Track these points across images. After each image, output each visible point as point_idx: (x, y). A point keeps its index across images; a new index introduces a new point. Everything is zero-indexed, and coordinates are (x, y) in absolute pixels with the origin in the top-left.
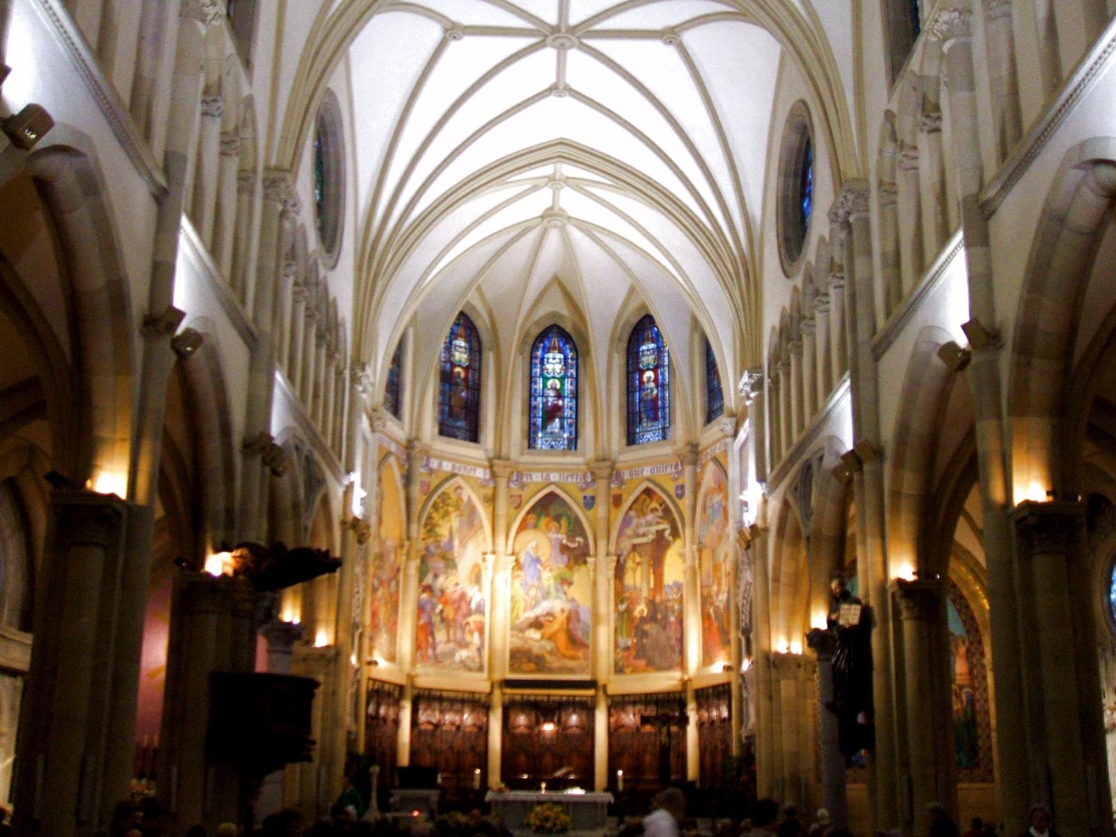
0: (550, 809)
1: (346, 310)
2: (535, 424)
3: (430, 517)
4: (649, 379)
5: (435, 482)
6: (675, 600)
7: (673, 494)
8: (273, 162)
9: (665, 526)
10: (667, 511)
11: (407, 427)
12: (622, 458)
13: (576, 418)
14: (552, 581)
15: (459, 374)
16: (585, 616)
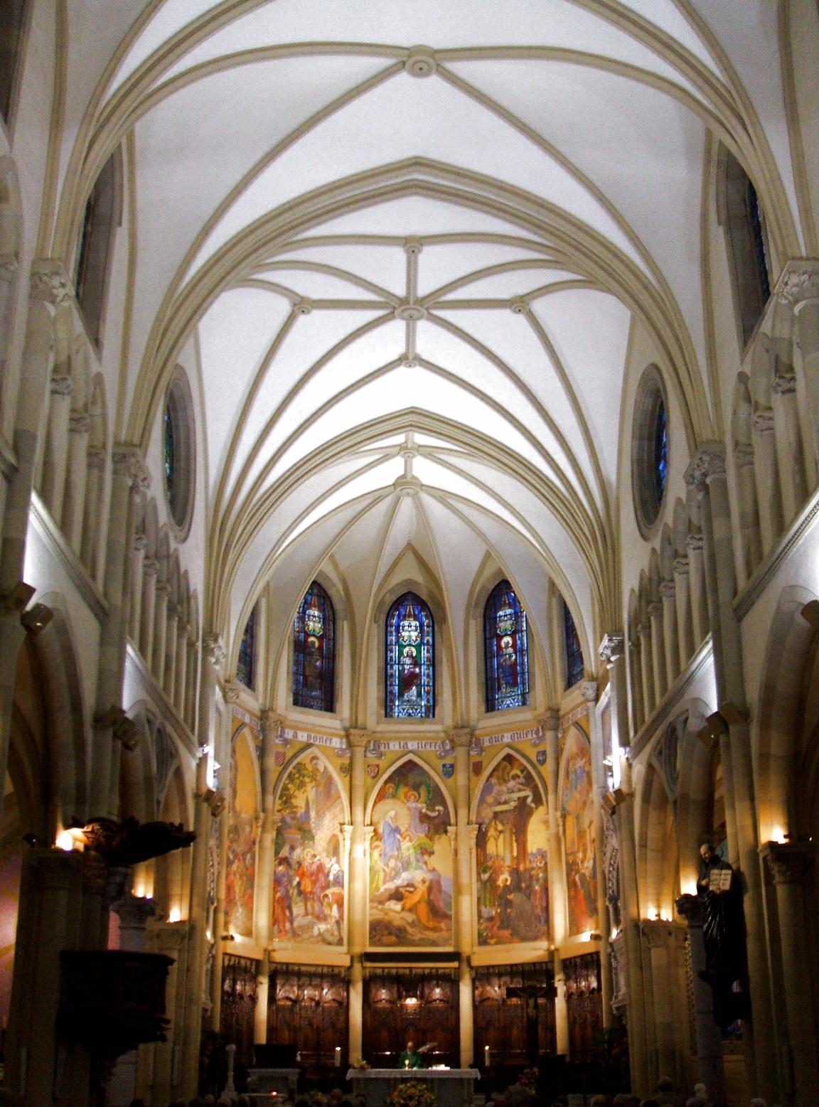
0: (413, 1086)
1: (197, 582)
2: (391, 692)
3: (285, 788)
4: (507, 646)
5: (290, 754)
6: (540, 868)
7: (534, 759)
8: (123, 437)
9: (528, 793)
10: (529, 777)
11: (261, 699)
13: (434, 686)
14: (411, 851)
15: (313, 643)
16: (447, 886)
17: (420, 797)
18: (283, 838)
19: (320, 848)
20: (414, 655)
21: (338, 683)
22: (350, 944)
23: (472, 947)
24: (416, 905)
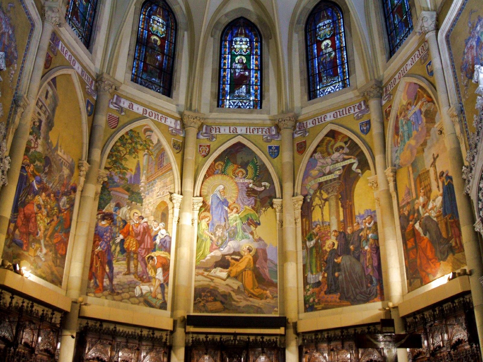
2: (224, 89)
3: (115, 149)
4: (326, 47)
9: (354, 161)
12: (304, 111)
13: (261, 85)
14: (239, 221)
16: (273, 255)
17: (247, 174)
18: (109, 194)
19: (148, 212)
20: (244, 62)
21: (176, 76)
22: (173, 309)
23: (298, 313)
24: (242, 272)
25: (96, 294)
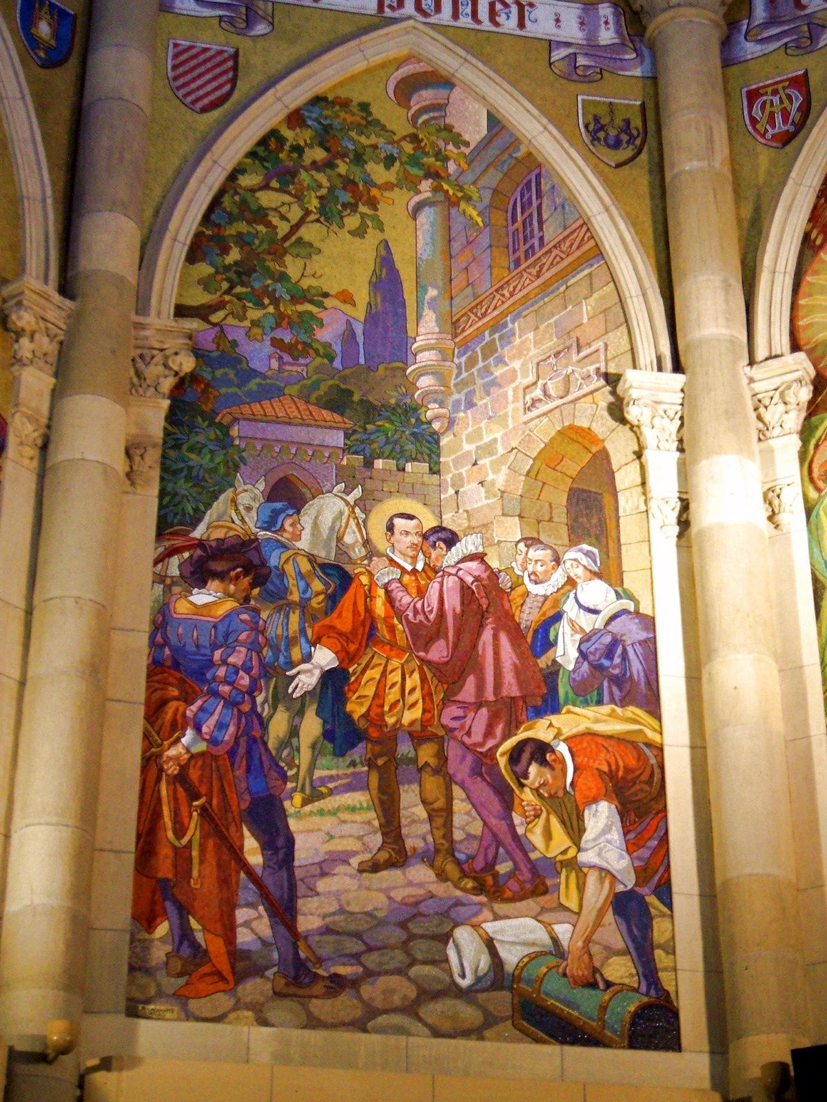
18: (225, 441)
19: (476, 498)
25: (193, 1005)
